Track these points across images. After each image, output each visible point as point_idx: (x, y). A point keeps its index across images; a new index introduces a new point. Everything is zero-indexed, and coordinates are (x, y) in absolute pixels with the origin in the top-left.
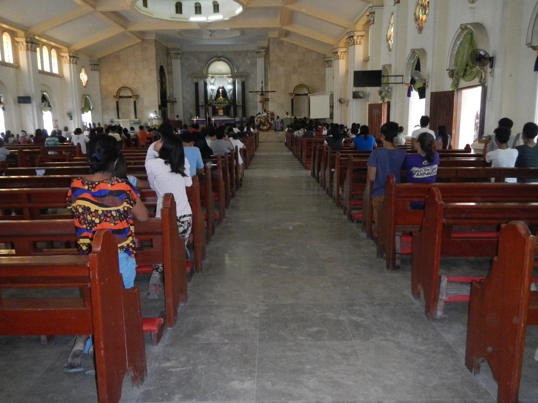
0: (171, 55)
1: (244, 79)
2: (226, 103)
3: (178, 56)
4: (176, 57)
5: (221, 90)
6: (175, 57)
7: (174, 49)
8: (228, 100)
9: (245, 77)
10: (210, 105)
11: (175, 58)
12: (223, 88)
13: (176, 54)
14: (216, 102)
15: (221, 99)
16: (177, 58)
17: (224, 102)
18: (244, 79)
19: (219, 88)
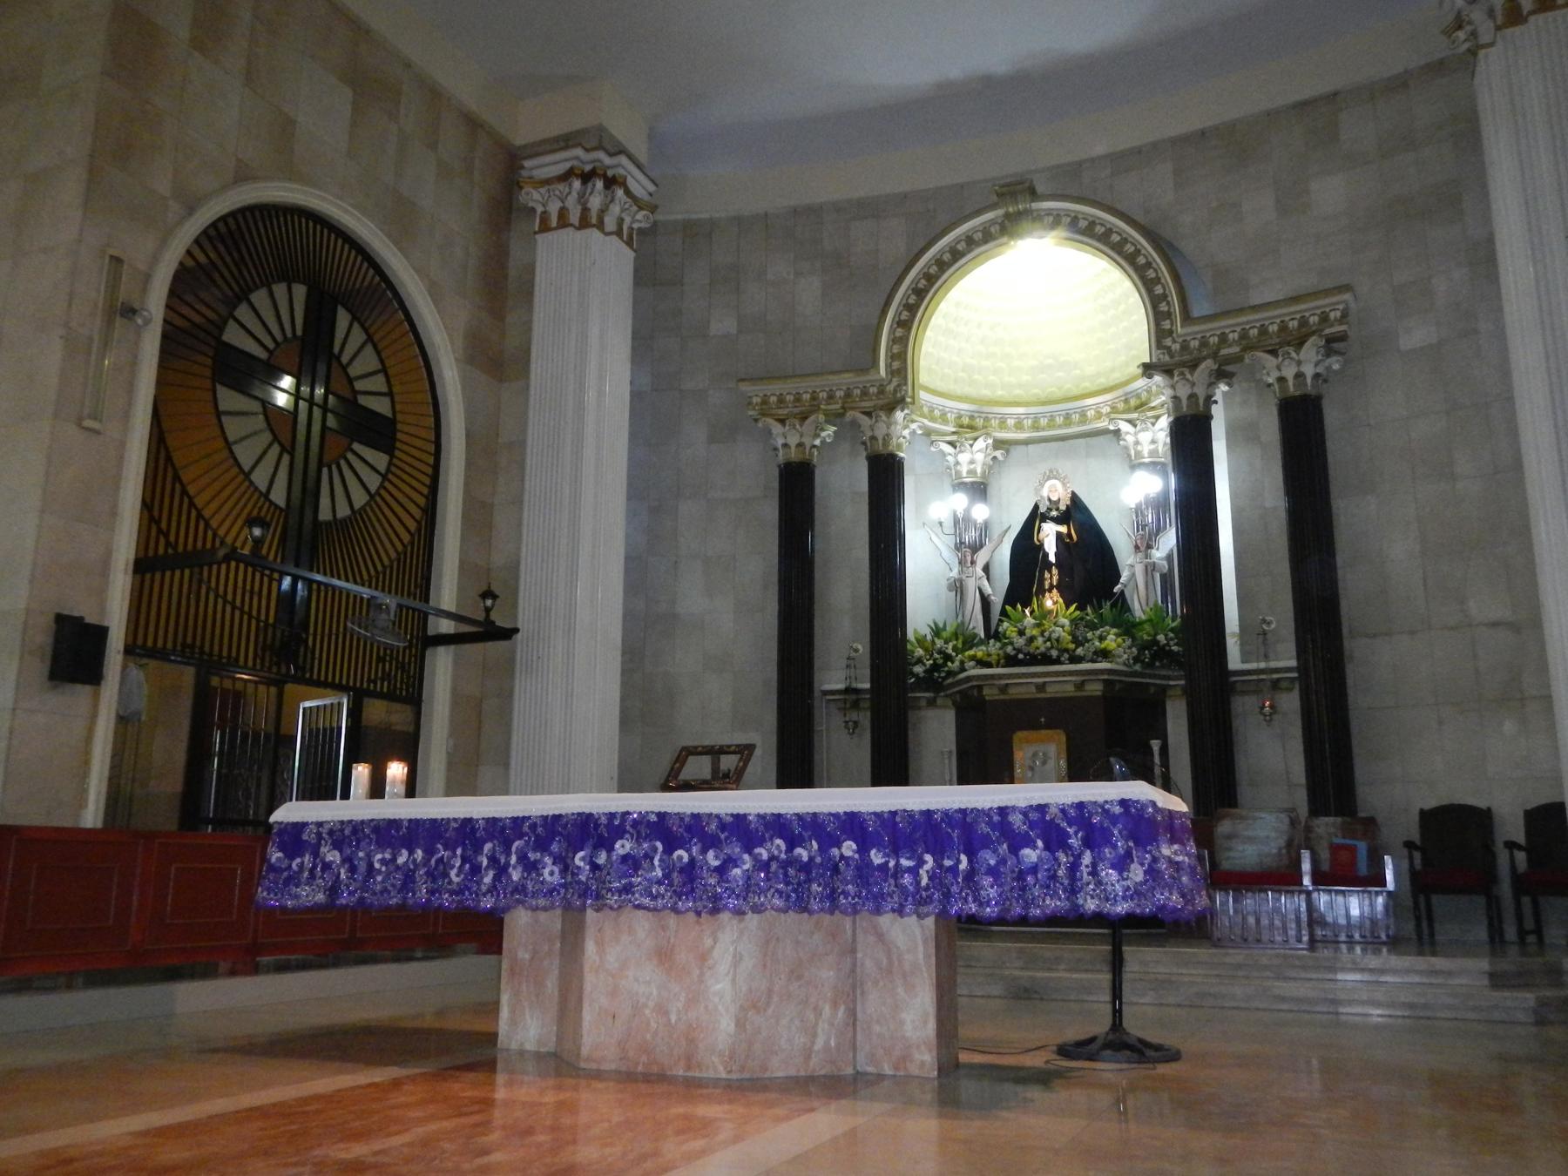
0: (532, 197)
1: (1309, 360)
2: (1105, 654)
3: (595, 202)
4: (574, 218)
5: (1049, 535)
6: (563, 213)
7: (566, 141)
8: (1128, 628)
9: (1332, 345)
10: (935, 680)
11: (563, 223)
12: (1075, 513)
13: (566, 177)
14: (994, 647)
15: (1046, 614)
16: (584, 223)
17: (1078, 642)
18: (1309, 360)
19: (1036, 517)
